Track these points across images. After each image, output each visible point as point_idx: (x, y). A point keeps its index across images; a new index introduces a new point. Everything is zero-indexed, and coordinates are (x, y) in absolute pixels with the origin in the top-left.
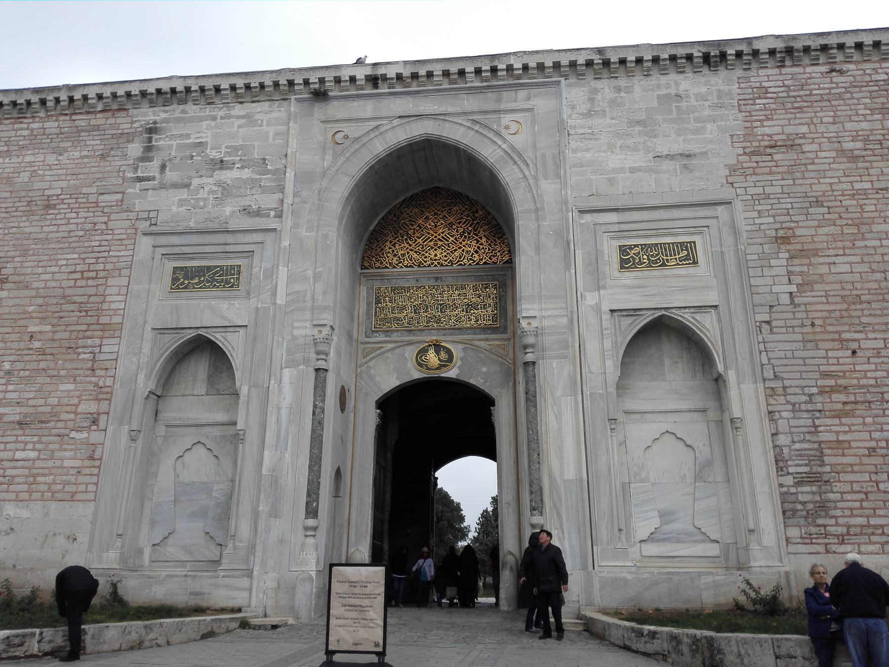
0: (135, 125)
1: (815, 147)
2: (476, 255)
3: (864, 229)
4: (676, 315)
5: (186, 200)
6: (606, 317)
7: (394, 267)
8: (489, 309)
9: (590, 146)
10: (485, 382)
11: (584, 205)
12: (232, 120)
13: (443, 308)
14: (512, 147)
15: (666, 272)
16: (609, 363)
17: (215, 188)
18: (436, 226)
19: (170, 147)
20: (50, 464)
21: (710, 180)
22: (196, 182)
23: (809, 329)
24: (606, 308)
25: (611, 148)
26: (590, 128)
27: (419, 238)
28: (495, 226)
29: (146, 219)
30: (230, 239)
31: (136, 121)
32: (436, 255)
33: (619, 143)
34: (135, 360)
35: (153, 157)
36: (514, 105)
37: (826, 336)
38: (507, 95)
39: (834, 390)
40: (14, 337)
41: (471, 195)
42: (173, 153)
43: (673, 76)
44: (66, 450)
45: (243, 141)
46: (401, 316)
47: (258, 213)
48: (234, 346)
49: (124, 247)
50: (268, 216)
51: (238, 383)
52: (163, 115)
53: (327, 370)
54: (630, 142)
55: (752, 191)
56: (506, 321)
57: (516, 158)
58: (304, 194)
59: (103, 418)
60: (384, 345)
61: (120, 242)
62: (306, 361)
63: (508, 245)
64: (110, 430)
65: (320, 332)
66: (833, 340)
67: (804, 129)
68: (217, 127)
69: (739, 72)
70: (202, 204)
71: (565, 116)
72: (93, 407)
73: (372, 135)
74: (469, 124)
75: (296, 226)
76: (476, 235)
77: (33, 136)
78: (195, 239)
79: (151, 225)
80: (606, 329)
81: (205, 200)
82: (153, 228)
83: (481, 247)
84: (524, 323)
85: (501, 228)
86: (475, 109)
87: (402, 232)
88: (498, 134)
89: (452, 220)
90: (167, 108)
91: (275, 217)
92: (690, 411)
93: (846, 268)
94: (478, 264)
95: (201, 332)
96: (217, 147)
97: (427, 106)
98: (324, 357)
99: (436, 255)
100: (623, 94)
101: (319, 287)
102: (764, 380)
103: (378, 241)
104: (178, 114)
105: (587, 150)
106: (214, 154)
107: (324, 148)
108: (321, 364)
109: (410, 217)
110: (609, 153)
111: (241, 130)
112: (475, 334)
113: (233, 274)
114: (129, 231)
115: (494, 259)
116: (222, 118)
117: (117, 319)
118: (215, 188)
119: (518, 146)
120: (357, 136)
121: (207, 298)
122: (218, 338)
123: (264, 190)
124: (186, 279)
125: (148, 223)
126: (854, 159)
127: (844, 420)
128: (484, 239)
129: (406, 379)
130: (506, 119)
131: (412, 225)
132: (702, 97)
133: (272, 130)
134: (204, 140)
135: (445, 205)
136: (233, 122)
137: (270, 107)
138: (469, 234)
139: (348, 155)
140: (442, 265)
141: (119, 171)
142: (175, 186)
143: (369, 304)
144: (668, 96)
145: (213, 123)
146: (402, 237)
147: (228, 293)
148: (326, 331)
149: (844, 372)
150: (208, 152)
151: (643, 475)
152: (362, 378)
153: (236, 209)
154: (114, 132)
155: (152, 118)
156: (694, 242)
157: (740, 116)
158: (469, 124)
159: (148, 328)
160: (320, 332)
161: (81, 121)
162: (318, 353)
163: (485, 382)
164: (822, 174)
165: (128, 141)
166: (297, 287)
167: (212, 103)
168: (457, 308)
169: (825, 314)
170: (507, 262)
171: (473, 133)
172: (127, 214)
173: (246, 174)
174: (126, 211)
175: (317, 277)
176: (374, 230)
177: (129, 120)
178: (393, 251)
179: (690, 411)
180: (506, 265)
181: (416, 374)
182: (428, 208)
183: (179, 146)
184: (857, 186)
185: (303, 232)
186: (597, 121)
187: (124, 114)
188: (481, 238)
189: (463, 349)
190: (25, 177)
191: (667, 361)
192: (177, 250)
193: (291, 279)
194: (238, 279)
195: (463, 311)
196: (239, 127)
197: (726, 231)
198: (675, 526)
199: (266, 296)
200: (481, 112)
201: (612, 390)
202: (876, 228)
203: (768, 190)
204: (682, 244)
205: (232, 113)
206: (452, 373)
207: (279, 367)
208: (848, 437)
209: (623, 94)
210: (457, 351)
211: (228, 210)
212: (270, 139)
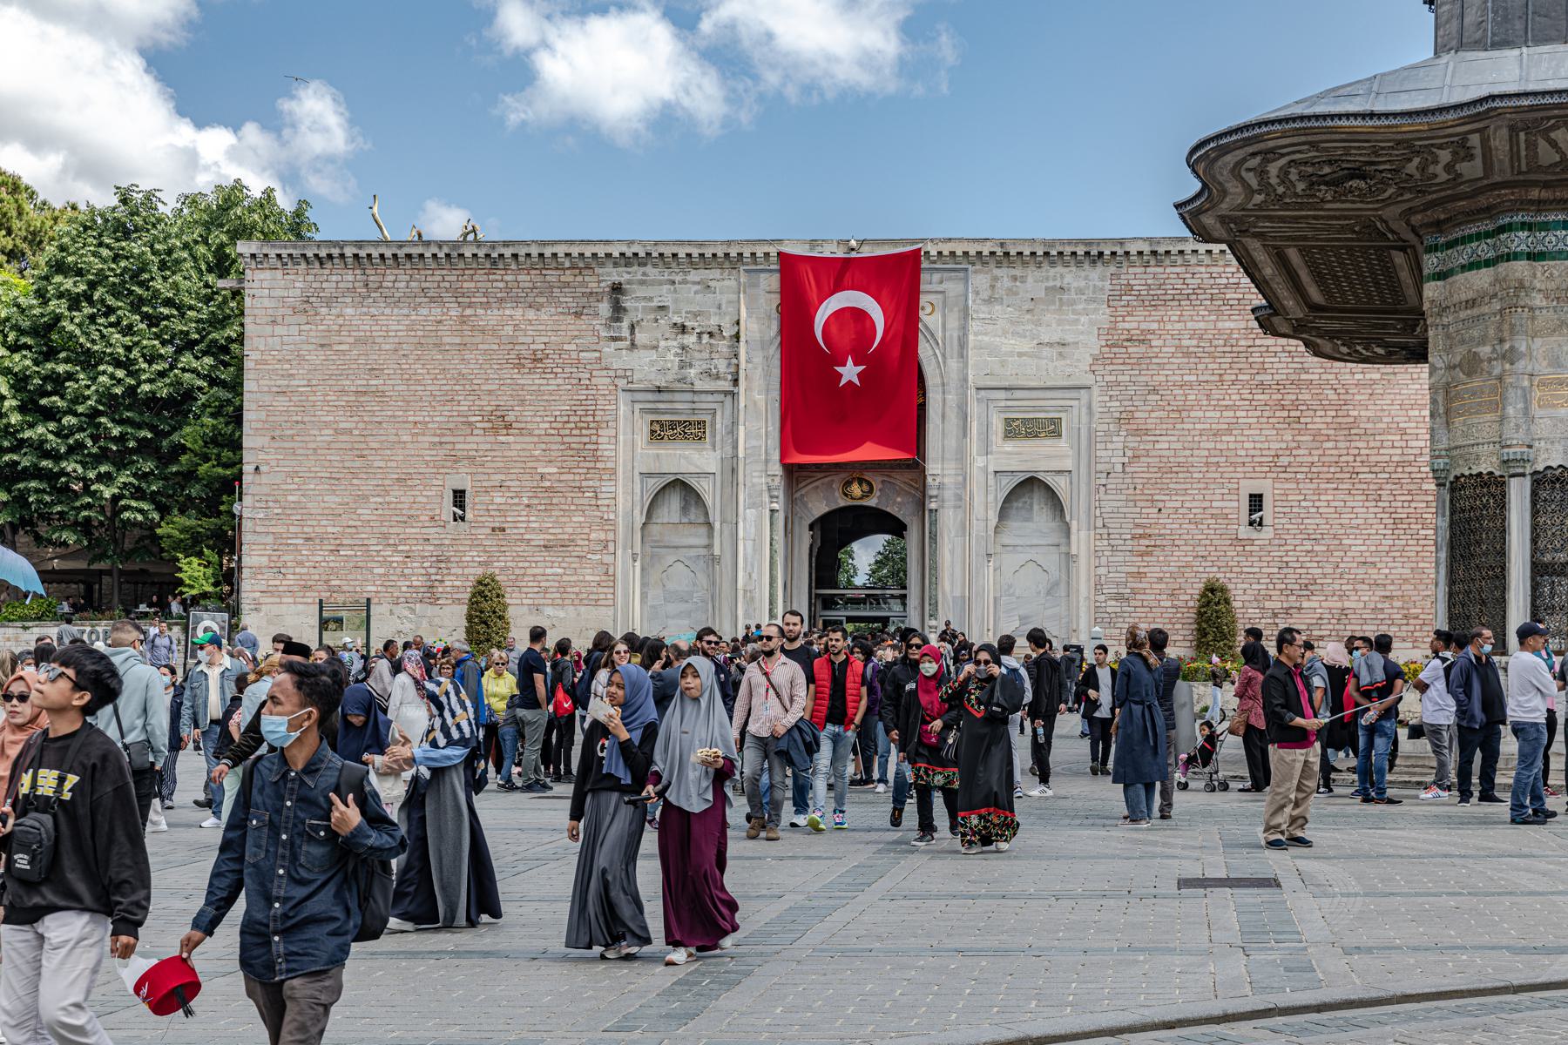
1: (1160, 343)
3: (1184, 414)
4: (1040, 476)
6: (991, 477)
11: (981, 384)
19: (636, 309)
20: (574, 578)
21: (1077, 367)
22: (662, 343)
23: (1131, 491)
24: (991, 469)
25: (1005, 333)
34: (625, 499)
39: (1141, 536)
40: (527, 477)
43: (1060, 269)
48: (705, 488)
54: (1020, 329)
55: (1107, 378)
59: (611, 545)
64: (619, 552)
67: (1155, 326)
69: (1112, 269)
72: (602, 536)
77: (508, 290)
93: (1166, 446)
96: (678, 312)
117: (610, 465)
122: (693, 482)
124: (661, 431)
126: (1187, 354)
132: (1080, 291)
142: (645, 347)
144: (1054, 288)
155: (616, 279)
157: (1108, 311)
161: (552, 276)
164: (1162, 366)
166: (754, 443)
181: (843, 502)
184: (1186, 378)
187: (589, 272)
190: (509, 330)
197: (1084, 410)
202: (1193, 414)
203: (1120, 378)
206: (872, 502)
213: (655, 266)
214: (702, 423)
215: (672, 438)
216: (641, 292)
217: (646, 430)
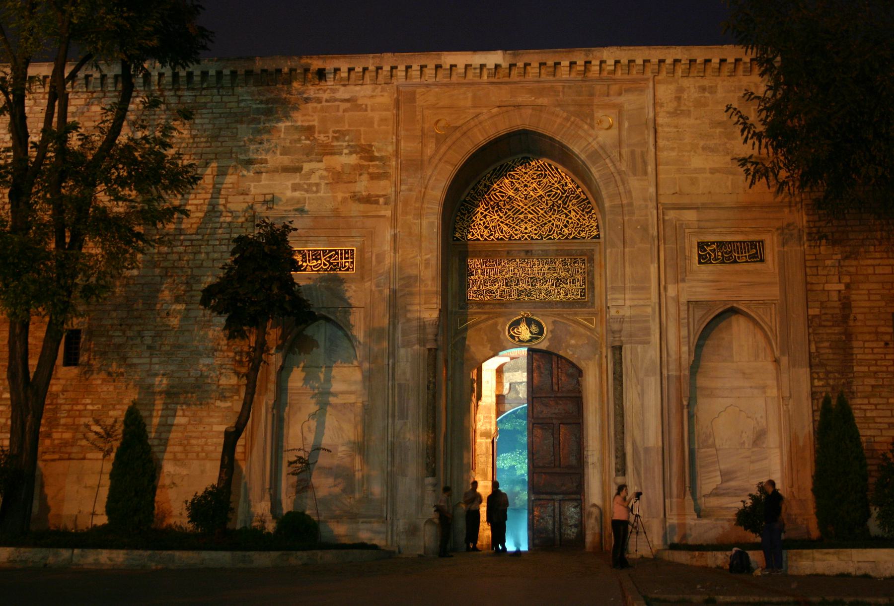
0: (242, 105)
2: (566, 230)
6: (684, 308)
8: (578, 284)
9: (676, 146)
12: (337, 103)
15: (736, 267)
16: (685, 349)
17: (325, 173)
22: (307, 167)
24: (683, 299)
26: (676, 127)
27: (509, 210)
28: (584, 200)
31: (243, 100)
32: (526, 228)
33: (702, 143)
37: (865, 329)
44: (211, 417)
50: (377, 202)
56: (593, 296)
66: (870, 333)
73: (472, 123)
76: (566, 209)
80: (684, 319)
81: (317, 185)
88: (593, 127)
89: (541, 193)
92: (751, 387)
94: (567, 238)
99: (526, 228)
100: (707, 94)
102: (811, 366)
103: (469, 213)
105: (673, 149)
110: (692, 153)
111: (347, 114)
113: (348, 258)
115: (583, 234)
116: (327, 101)
120: (457, 125)
123: (373, 177)
127: (872, 401)
128: (573, 213)
131: (503, 197)
134: (311, 123)
135: (535, 176)
136: (338, 106)
138: (558, 207)
140: (532, 239)
142: (286, 170)
145: (319, 106)
146: (493, 208)
149: (876, 360)
151: (710, 441)
156: (762, 242)
165: (237, 122)
169: (867, 310)
170: (595, 237)
172: (242, 197)
173: (353, 159)
174: (242, 194)
177: (234, 99)
179: (751, 387)
186: (684, 121)
188: (570, 212)
191: (735, 346)
198: (733, 484)
201: (687, 372)
204: (752, 242)
205: (339, 95)
208: (874, 414)
209: (707, 94)
211: (340, 196)
212: (376, 126)
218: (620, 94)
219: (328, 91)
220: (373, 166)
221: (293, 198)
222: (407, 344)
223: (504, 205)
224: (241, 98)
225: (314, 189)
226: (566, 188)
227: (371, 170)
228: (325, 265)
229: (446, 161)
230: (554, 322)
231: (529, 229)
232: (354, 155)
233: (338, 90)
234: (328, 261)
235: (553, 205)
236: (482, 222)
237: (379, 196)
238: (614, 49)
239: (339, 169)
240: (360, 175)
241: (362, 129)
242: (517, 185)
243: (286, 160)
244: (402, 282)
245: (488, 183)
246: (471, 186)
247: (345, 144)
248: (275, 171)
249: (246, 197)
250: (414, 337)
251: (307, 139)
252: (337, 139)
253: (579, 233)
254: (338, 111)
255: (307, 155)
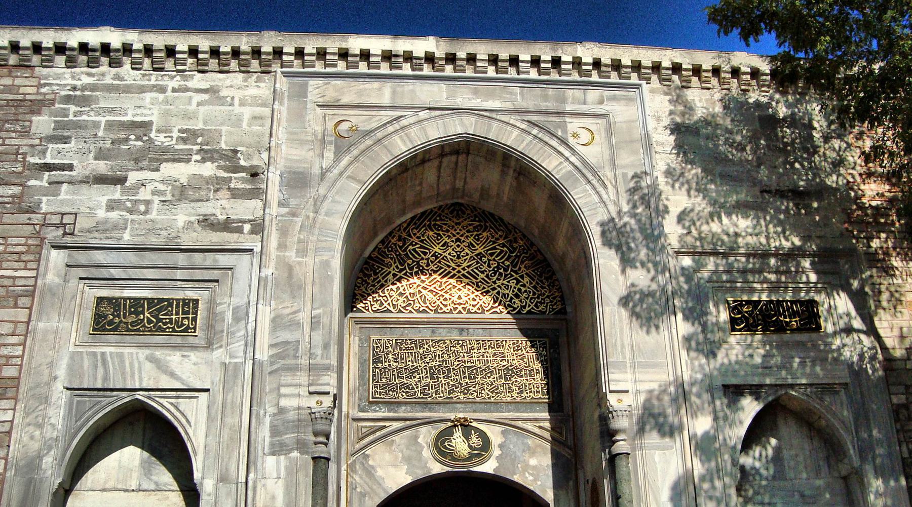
0: (43, 90)
2: (517, 301)
5: (119, 201)
7: (400, 311)
10: (535, 480)
12: (189, 94)
13: (472, 373)
14: (584, 162)
18: (459, 257)
19: (96, 125)
22: (133, 177)
29: (57, 226)
30: (181, 259)
31: (45, 85)
32: (460, 297)
35: (69, 137)
36: (582, 108)
38: (572, 93)
41: (507, 217)
42: (101, 134)
45: (205, 123)
46: (413, 382)
47: (227, 226)
49: (22, 265)
50: (240, 230)
51: (197, 476)
52: (86, 80)
53: (328, 459)
57: (590, 177)
58: (293, 202)
60: (387, 424)
61: (16, 257)
62: (301, 446)
63: (560, 289)
65: (320, 403)
68: (166, 101)
70: (142, 208)
71: (650, 128)
74: (524, 126)
75: (282, 246)
76: (517, 274)
78: (131, 258)
79: (65, 234)
81: (148, 203)
82: (68, 239)
83: (523, 289)
84: (612, 399)
85: (549, 265)
86: (531, 108)
87: (410, 262)
88: (564, 142)
90: (93, 71)
91: (252, 232)
95: (140, 396)
97: (465, 97)
98: (322, 439)
99: (460, 297)
101: (318, 337)
103: (376, 274)
104: (108, 80)
106: (160, 139)
107: (323, 142)
108: (320, 451)
109: (422, 241)
111: (202, 109)
112: (518, 411)
114: (30, 242)
118: (162, 187)
119: (592, 160)
120: (368, 128)
121: (148, 346)
122: (164, 405)
123: (236, 194)
125: (60, 232)
128: (527, 279)
129: (420, 474)
130: (574, 125)
131: (425, 254)
133: (247, 112)
134: (146, 119)
136: (191, 98)
137: (245, 80)
138: (506, 270)
139: (355, 152)
140: (469, 312)
141: (17, 153)
142: (101, 180)
143: (362, 363)
145: (161, 97)
146: (411, 269)
147: (179, 340)
148: (327, 401)
150: (153, 135)
152: (355, 472)
153: (192, 219)
154: (10, 97)
158: (524, 126)
159: (59, 386)
160: (320, 403)
162: (316, 434)
163: (535, 480)
165: (33, 112)
167: (162, 69)
168: (491, 372)
171: (530, 138)
172: (28, 215)
173: (209, 169)
174: (27, 212)
175: (315, 323)
176: (370, 257)
177: (34, 82)
178: (398, 288)
180: (559, 316)
181: (437, 468)
182: (448, 231)
183: (110, 125)
185: (291, 255)
188: (522, 277)
189: (503, 433)
192: (104, 273)
193: (277, 323)
194: (195, 319)
195: (500, 377)
196: (199, 104)
199: (238, 347)
200: (540, 112)
205: (190, 84)
206: (488, 467)
207: (260, 453)
210: (494, 434)
211: (181, 219)
212: (245, 125)
213: (136, 66)
214: (190, 305)
215: (135, 329)
216: (105, 101)
217: (89, 315)
218: (601, 102)
219: (178, 78)
220: (235, 178)
221: (106, 221)
222: (278, 449)
223: (428, 265)
224: (42, 82)
225: (142, 208)
226: (515, 245)
227: (232, 185)
228: (150, 322)
229: (349, 177)
230: (503, 433)
231: (465, 299)
232: (209, 163)
233: (192, 77)
234: (156, 317)
235: (498, 267)
236: (394, 287)
237: (244, 222)
238: (589, 45)
239: (184, 181)
240: (216, 191)
241: (224, 129)
242: (446, 239)
243: (102, 167)
244: (274, 351)
245: (404, 235)
246: (380, 237)
247: (198, 147)
248: (85, 181)
249: (32, 216)
250: (289, 437)
251: (138, 139)
252: (184, 140)
253: (536, 305)
254: (190, 103)
255: (137, 161)
